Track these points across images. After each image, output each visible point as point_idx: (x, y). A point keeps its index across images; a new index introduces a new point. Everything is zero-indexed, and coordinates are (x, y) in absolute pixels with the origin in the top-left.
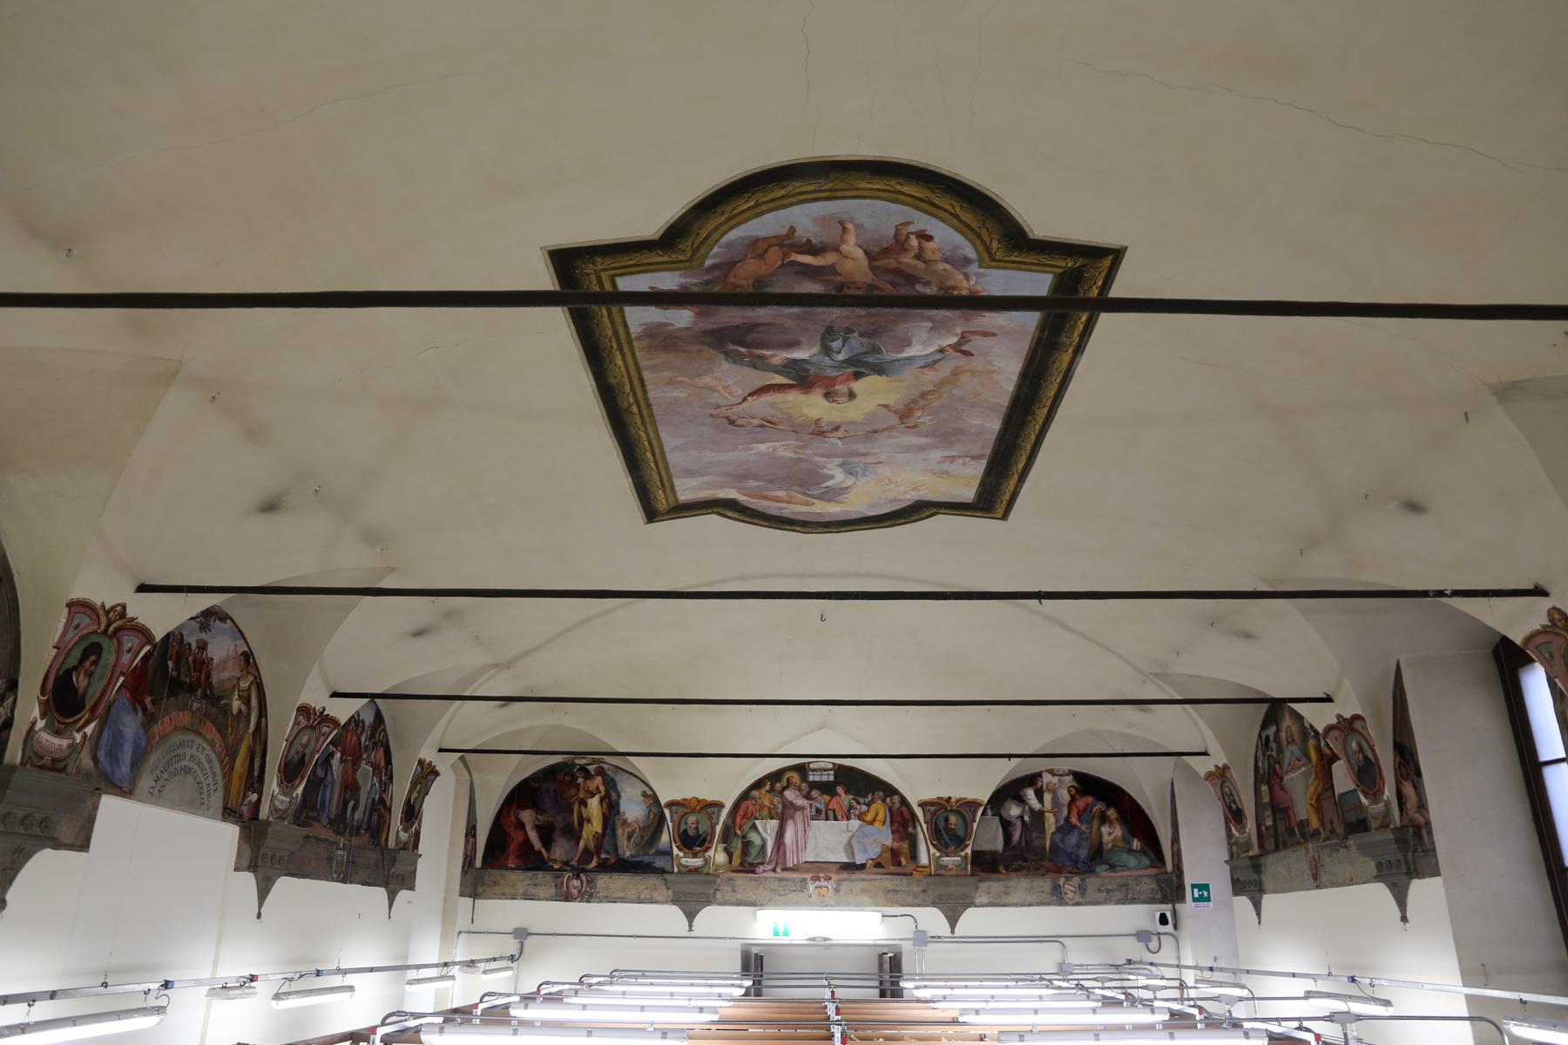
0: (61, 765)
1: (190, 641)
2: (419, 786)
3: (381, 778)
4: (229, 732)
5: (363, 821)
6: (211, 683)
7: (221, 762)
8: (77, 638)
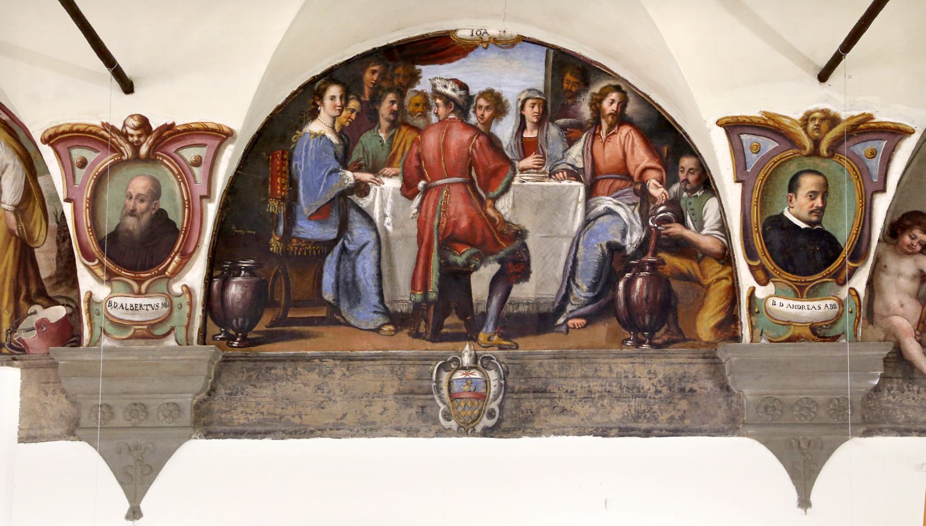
3: (644, 197)
5: (565, 299)
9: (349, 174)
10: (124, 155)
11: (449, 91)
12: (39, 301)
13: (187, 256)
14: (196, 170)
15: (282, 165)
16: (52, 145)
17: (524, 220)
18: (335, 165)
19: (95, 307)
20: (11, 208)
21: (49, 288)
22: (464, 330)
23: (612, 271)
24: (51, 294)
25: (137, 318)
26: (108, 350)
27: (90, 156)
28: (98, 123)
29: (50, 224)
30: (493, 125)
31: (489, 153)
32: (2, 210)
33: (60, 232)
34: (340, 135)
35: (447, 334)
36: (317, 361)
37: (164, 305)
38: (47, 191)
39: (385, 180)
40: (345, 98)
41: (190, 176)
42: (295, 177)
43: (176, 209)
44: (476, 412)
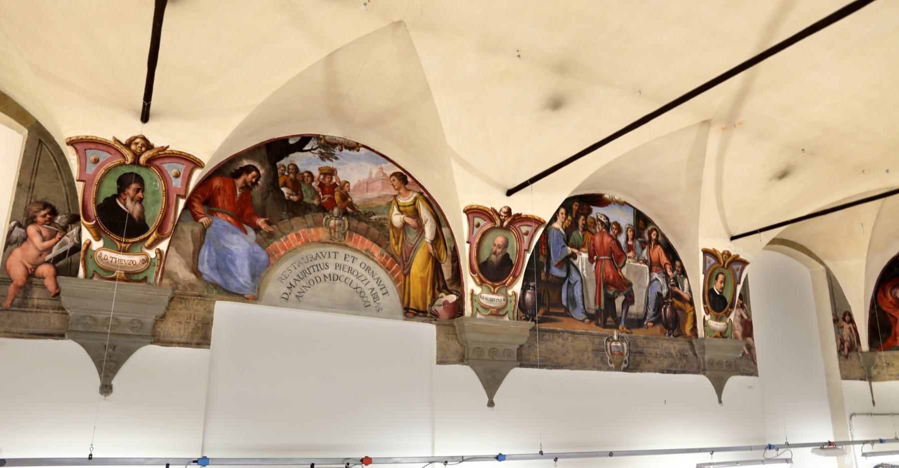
0: (141, 277)
1: (310, 169)
2: (721, 277)
3: (666, 273)
4: (393, 241)
6: (351, 202)
7: (388, 269)
8: (102, 171)
9: (569, 248)
10: (496, 224)
11: (602, 219)
12: (444, 291)
13: (515, 278)
14: (525, 237)
15: (544, 240)
16: (467, 215)
17: (631, 278)
18: (564, 243)
19: (474, 298)
20: (429, 241)
22: (614, 324)
23: (659, 303)
24: (449, 288)
25: (492, 305)
26: (480, 319)
27: (482, 222)
28: (490, 208)
29: (448, 252)
30: (618, 236)
31: (617, 248)
32: (425, 243)
34: (565, 230)
35: (608, 325)
36: (561, 333)
37: (504, 300)
39: (583, 254)
40: (567, 214)
41: (522, 241)
42: (549, 246)
43: (513, 255)
44: (621, 361)
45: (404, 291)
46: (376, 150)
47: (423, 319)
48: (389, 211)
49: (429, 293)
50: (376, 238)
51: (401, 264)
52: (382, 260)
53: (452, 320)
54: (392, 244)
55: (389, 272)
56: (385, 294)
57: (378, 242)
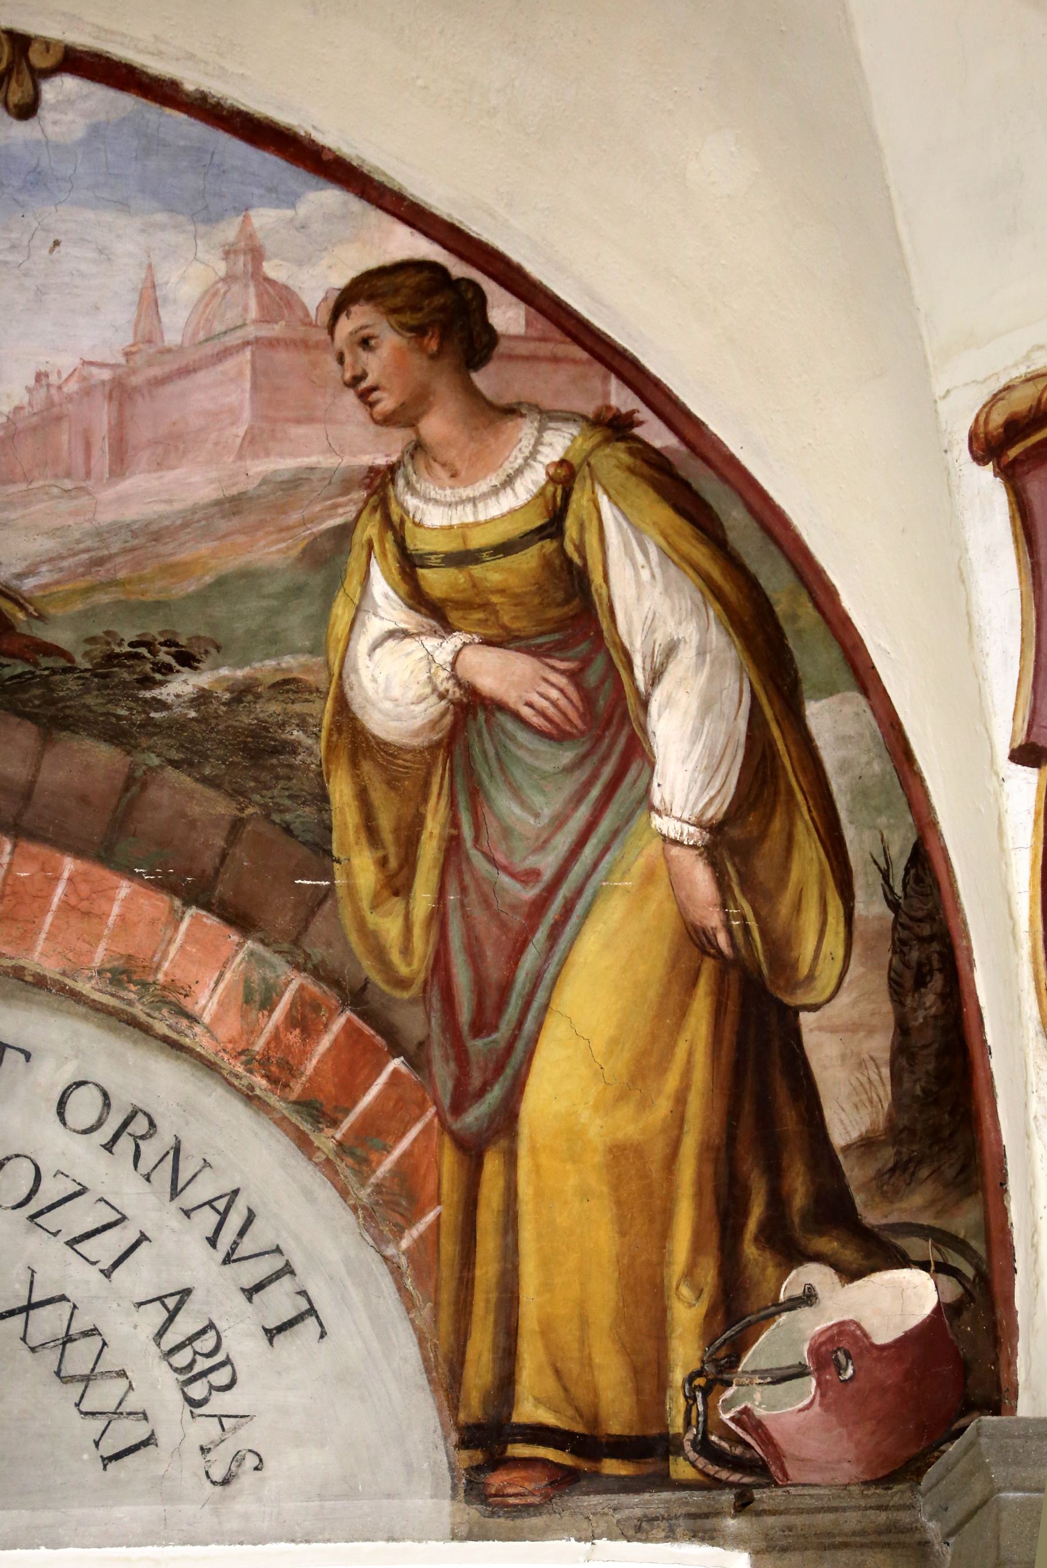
20: (691, 834)
21: (864, 1187)
24: (872, 1217)
32: (656, 845)
33: (903, 942)
38: (844, 766)
45: (466, 1284)
46: (192, 81)
47: (636, 1504)
48: (323, 618)
49: (689, 1273)
50: (208, 861)
51: (436, 1053)
52: (259, 1045)
53: (898, 1493)
54: (352, 889)
55: (326, 1140)
56: (281, 1329)
57: (221, 890)
